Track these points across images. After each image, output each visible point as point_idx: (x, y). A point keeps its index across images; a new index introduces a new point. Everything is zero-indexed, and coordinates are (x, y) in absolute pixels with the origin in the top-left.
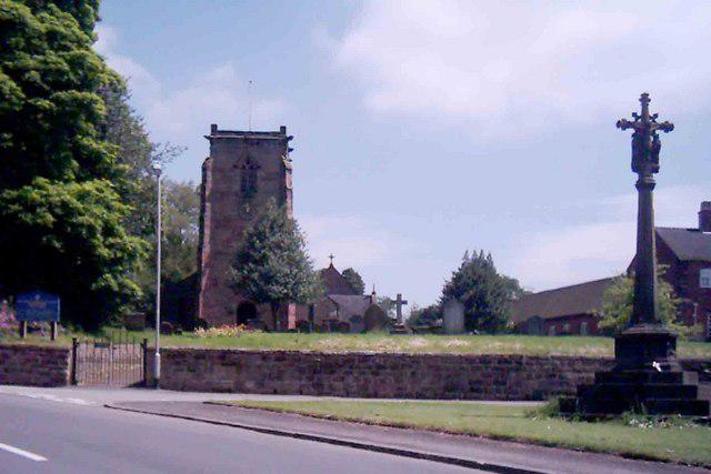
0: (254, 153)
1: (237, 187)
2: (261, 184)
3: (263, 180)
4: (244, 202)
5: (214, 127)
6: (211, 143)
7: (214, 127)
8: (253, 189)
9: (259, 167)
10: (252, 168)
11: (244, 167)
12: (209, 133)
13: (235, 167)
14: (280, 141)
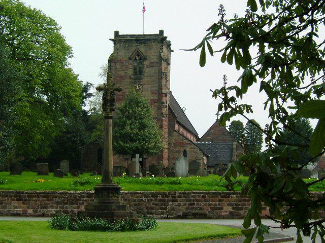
0: (142, 49)
1: (130, 72)
2: (146, 71)
3: (147, 67)
4: (135, 83)
5: (117, 33)
6: (114, 43)
7: (117, 33)
8: (141, 72)
9: (145, 59)
10: (140, 59)
11: (136, 59)
12: (113, 37)
13: (130, 59)
14: (118, 39)
